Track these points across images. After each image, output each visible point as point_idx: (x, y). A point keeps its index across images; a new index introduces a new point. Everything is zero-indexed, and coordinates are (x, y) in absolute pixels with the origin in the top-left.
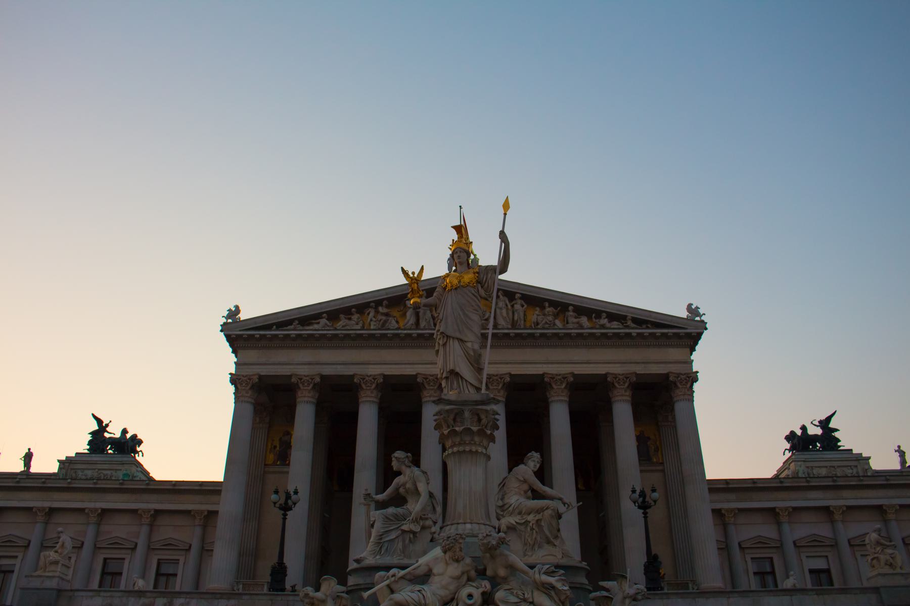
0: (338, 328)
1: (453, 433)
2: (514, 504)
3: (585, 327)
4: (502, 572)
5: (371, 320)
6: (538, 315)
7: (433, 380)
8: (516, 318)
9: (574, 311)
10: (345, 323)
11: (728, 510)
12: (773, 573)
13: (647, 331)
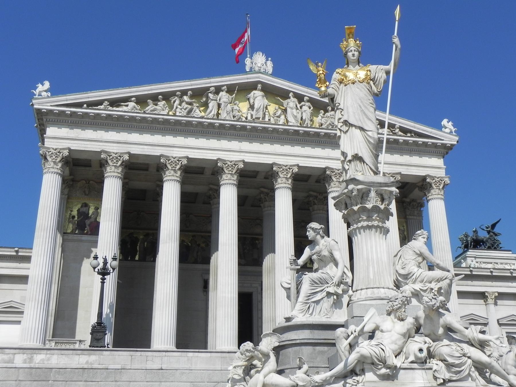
0: (147, 112)
1: (364, 210)
2: (416, 274)
5: (177, 108)
6: (322, 117)
7: (232, 166)
8: (304, 118)
10: (153, 108)
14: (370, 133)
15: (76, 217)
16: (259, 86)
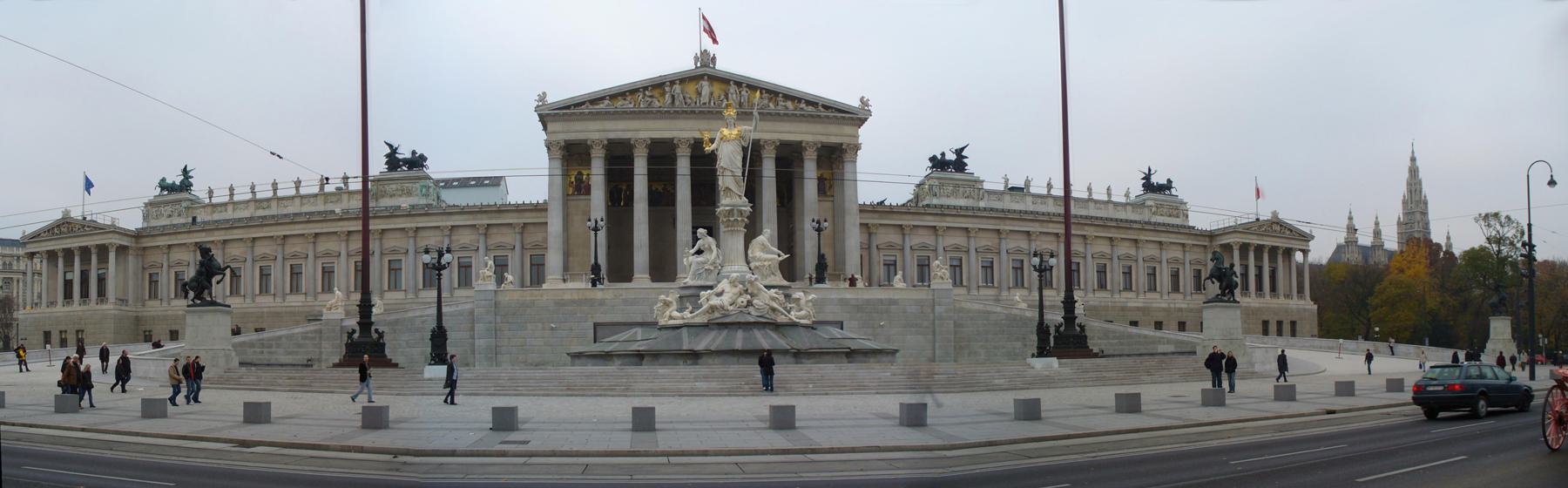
4: (755, 292)
9: (783, 97)
11: (872, 224)
12: (895, 265)
16: (706, 77)
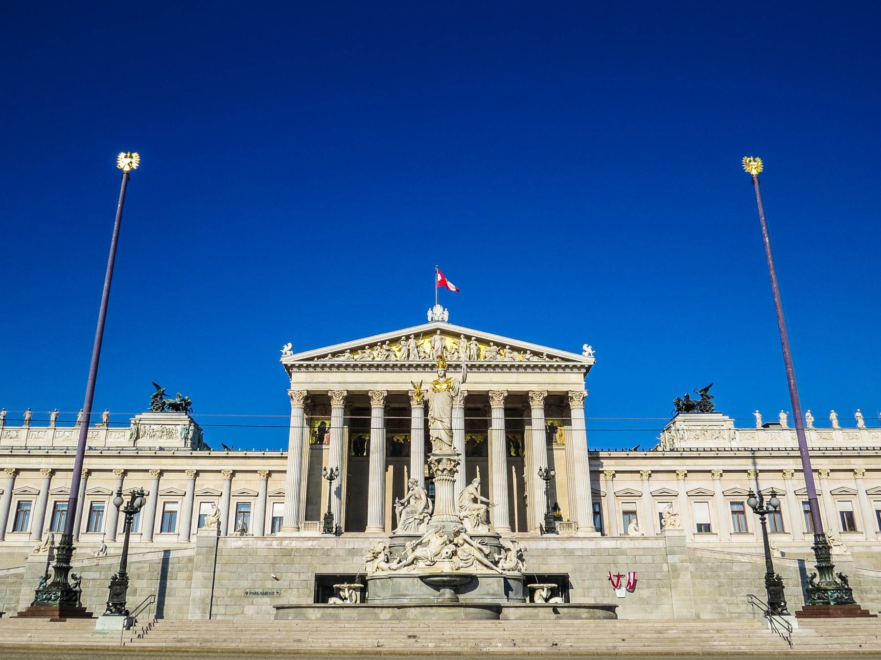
3: (516, 360)
13: (556, 364)
14: (446, 423)
15: (318, 432)
16: (438, 332)
